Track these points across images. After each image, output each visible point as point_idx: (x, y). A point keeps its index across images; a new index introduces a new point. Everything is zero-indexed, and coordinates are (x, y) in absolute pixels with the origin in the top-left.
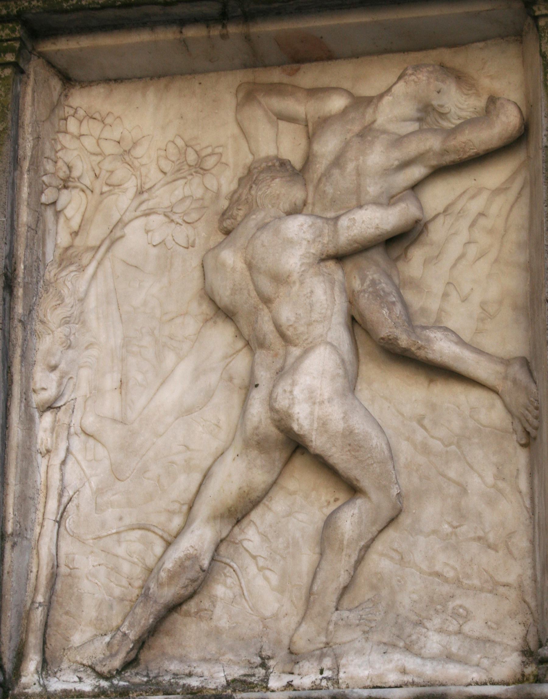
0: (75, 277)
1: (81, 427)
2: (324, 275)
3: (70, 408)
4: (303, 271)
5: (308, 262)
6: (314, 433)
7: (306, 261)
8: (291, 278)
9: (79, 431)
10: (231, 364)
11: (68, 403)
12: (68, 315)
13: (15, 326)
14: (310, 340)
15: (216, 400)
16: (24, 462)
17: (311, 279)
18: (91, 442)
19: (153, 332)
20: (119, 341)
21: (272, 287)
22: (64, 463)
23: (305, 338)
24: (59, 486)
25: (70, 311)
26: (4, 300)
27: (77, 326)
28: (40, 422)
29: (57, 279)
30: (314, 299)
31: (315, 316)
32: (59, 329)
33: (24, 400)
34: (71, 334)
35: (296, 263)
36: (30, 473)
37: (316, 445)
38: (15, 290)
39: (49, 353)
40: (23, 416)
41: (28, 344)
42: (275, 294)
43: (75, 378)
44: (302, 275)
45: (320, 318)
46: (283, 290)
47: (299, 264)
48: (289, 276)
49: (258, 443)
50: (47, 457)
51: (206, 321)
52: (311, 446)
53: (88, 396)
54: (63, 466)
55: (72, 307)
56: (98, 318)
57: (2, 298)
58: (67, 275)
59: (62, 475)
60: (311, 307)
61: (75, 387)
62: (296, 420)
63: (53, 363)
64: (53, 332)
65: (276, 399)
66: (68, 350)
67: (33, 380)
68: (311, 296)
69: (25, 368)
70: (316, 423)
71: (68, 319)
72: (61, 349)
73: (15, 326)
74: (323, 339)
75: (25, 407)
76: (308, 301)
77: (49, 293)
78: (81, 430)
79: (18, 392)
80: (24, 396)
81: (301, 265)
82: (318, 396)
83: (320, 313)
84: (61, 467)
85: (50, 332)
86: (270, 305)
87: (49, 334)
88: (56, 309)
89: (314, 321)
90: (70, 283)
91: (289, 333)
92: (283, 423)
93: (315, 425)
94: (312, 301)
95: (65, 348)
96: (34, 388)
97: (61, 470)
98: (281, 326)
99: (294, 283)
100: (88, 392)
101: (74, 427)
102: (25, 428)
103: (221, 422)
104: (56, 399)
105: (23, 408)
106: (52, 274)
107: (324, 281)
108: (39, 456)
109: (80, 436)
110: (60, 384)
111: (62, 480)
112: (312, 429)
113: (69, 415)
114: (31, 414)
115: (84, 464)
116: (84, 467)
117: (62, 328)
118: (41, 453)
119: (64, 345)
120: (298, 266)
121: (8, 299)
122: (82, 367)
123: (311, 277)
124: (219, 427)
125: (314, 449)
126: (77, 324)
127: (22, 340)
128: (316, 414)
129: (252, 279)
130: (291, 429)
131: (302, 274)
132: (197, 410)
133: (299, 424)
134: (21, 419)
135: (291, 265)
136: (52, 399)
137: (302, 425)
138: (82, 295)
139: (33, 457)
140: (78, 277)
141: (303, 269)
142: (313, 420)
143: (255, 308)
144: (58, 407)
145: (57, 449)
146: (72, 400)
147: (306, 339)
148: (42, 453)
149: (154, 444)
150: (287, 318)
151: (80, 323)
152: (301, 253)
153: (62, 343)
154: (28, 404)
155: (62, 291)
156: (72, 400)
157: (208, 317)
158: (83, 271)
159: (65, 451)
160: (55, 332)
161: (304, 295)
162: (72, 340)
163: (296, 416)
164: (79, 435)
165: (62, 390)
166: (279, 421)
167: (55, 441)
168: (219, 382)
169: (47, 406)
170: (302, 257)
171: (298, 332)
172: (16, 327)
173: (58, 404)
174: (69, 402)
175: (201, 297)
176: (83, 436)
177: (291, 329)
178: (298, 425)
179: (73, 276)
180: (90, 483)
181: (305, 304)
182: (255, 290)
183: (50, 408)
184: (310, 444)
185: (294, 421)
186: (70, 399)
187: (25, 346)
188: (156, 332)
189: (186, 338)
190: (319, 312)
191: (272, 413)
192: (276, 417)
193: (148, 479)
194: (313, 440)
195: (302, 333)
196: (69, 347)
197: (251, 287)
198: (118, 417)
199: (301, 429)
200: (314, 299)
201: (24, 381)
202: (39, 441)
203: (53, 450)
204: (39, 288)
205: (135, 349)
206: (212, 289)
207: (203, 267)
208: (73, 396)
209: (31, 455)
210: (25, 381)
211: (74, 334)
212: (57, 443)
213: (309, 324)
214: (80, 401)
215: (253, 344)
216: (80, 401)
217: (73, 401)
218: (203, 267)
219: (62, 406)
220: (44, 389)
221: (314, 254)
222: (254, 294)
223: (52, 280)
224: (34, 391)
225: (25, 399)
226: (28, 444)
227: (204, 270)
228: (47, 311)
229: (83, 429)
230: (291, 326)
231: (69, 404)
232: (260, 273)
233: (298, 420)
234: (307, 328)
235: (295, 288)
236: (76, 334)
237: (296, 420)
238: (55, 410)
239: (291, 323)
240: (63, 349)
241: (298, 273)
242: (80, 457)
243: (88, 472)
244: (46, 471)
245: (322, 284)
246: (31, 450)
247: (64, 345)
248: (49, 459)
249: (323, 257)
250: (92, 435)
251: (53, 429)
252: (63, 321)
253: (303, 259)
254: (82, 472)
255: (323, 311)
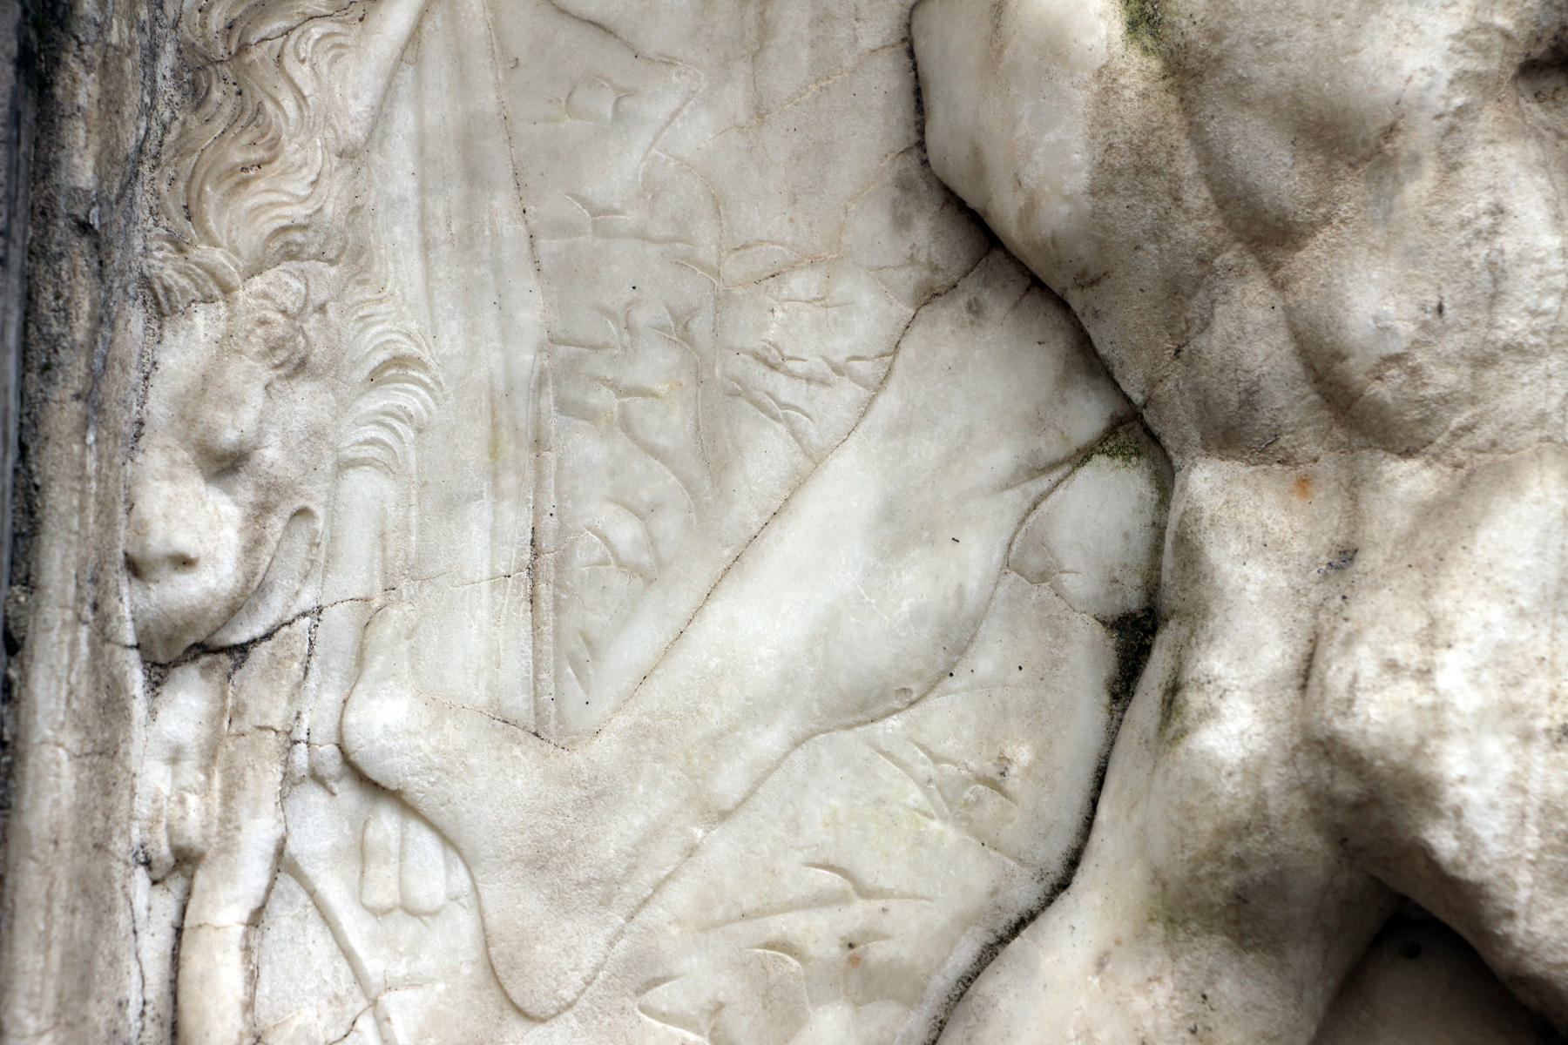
0: (327, 43)
1: (340, 747)
2: (1540, 137)
3: (293, 657)
4: (1461, 111)
5: (1481, 68)
6: (1524, 877)
7: (1473, 64)
8: (1399, 140)
9: (332, 766)
10: (1044, 507)
11: (285, 629)
12: (301, 220)
13: (55, 249)
14: (1487, 432)
15: (985, 662)
16: (79, 916)
17: (1490, 148)
18: (386, 824)
19: (685, 327)
20: (527, 359)
21: (1303, 174)
22: (256, 919)
23: (1457, 421)
24: (241, 1034)
25: (306, 199)
26: (16, 118)
27: (333, 271)
28: (153, 713)
29: (243, 48)
30: (1509, 244)
31: (1513, 324)
32: (258, 283)
33: (87, 613)
34: (310, 309)
35: (1432, 73)
36: (101, 964)
37: (1530, 933)
38: (63, 78)
39: (205, 386)
40: (83, 690)
41: (111, 342)
42: (1314, 205)
43: (320, 512)
44: (1452, 129)
45: (1535, 333)
46: (1352, 192)
47: (1447, 73)
48: (1391, 131)
49: (1240, 899)
50: (176, 885)
51: (929, 296)
52: (1506, 940)
53: (376, 604)
54: (253, 933)
55: (314, 183)
56: (427, 246)
57: (6, 109)
58: (287, 32)
59: (253, 978)
60: (1495, 282)
61: (325, 556)
62: (1450, 814)
63: (229, 437)
64: (227, 290)
65: (1350, 702)
66: (293, 383)
67: (129, 511)
68: (1494, 231)
69: (99, 458)
70: (1536, 831)
71: (298, 237)
72: (267, 375)
73: (55, 249)
74: (1545, 433)
75: (92, 643)
76: (1482, 250)
77: (209, 109)
78: (338, 760)
79: (63, 569)
80: (90, 592)
81: (1452, 82)
82: (1542, 701)
83: (1534, 313)
84: (246, 936)
85: (217, 292)
86: (1276, 255)
87: (208, 299)
88: (246, 182)
89: (1506, 348)
90: (306, 68)
91: (1382, 391)
92: (1377, 815)
93: (1532, 840)
94: (1502, 252)
95: (281, 372)
96: (134, 551)
97: (247, 949)
98: (1339, 356)
99: (1416, 159)
100: (378, 584)
101: (308, 744)
102: (88, 748)
103: (1013, 770)
104: (236, 609)
105: (84, 649)
106: (217, 20)
107: (1545, 165)
108: (141, 877)
109: (336, 789)
110: (253, 545)
111: (249, 1006)
112: (1518, 858)
113: (286, 687)
114: (114, 680)
115: (355, 927)
116: (356, 941)
117: (270, 274)
118: (148, 864)
119: (282, 355)
120: (1442, 84)
121: (29, 114)
122: (353, 464)
123: (1492, 142)
124: (1005, 794)
125: (1521, 951)
126: (331, 262)
127: (91, 318)
128: (1535, 786)
129: (1195, 131)
130: (1425, 854)
131: (1456, 123)
132: (896, 704)
133: (1462, 834)
134: (75, 705)
135: (1410, 79)
136: (217, 609)
137: (1475, 837)
138: (356, 133)
139: (118, 886)
140: (340, 46)
141: (1458, 101)
142: (1524, 816)
143: (1202, 261)
144: (235, 647)
145: (228, 846)
146: (304, 614)
147: (1468, 429)
148: (155, 864)
149: (692, 851)
150: (1376, 319)
151: (344, 258)
152: (1457, 28)
153: (272, 349)
154: (102, 630)
155: (269, 106)
156: (304, 614)
157: (940, 280)
158: (361, 20)
159: (270, 859)
160: (240, 294)
161: (1463, 225)
162: (311, 334)
163: (1452, 795)
164: (331, 784)
165: (262, 569)
166: (1358, 807)
167: (217, 809)
168: (997, 584)
169: (190, 640)
170: (1460, 45)
171: (1430, 392)
172: (61, 255)
173: (242, 636)
174: (289, 624)
175: (904, 185)
176: (347, 794)
177: (1394, 372)
178: (1457, 838)
179: (318, 41)
180: (382, 1021)
181: (1468, 264)
182: (1208, 178)
183: (202, 649)
184: (1504, 928)
185: (1438, 814)
186: (296, 610)
187: (100, 347)
188: (700, 326)
189: (837, 370)
190: (1532, 305)
191: (1324, 769)
192: (1346, 787)
193: (665, 1018)
194: (1516, 908)
195: (1448, 400)
196: (300, 367)
197: (1188, 166)
198: (519, 703)
199: (1471, 856)
200: (1509, 244)
201: (91, 520)
202: (143, 807)
203: (209, 855)
204: (159, 79)
205: (602, 398)
206: (977, 152)
207: (911, 53)
208: (307, 600)
209: (108, 878)
210: (95, 522)
211: (322, 309)
212: (228, 822)
213: (1483, 360)
214: (339, 624)
215: (1178, 423)
216: (339, 624)
217: (306, 621)
218: (911, 53)
219: (254, 642)
220: (184, 562)
221: (1507, 36)
222: (1197, 196)
223: (220, 50)
224: (135, 568)
225: (95, 607)
226: (99, 823)
227: (915, 67)
228: (201, 192)
229: (356, 758)
230: (1396, 359)
231: (287, 635)
232: (1246, 103)
233: (1458, 813)
234: (1473, 376)
235: (1418, 190)
236: (332, 310)
237: (1450, 814)
238: (223, 657)
239: (1397, 347)
240: (273, 373)
241: (1439, 117)
242: (334, 890)
243: (374, 966)
244: (169, 952)
245: (1541, 180)
246: (107, 851)
247: (282, 355)
248: (188, 893)
249: (1539, 51)
250: (393, 787)
251: (211, 753)
252: (276, 245)
253: (1463, 52)
254: (344, 967)
255: (1550, 303)
